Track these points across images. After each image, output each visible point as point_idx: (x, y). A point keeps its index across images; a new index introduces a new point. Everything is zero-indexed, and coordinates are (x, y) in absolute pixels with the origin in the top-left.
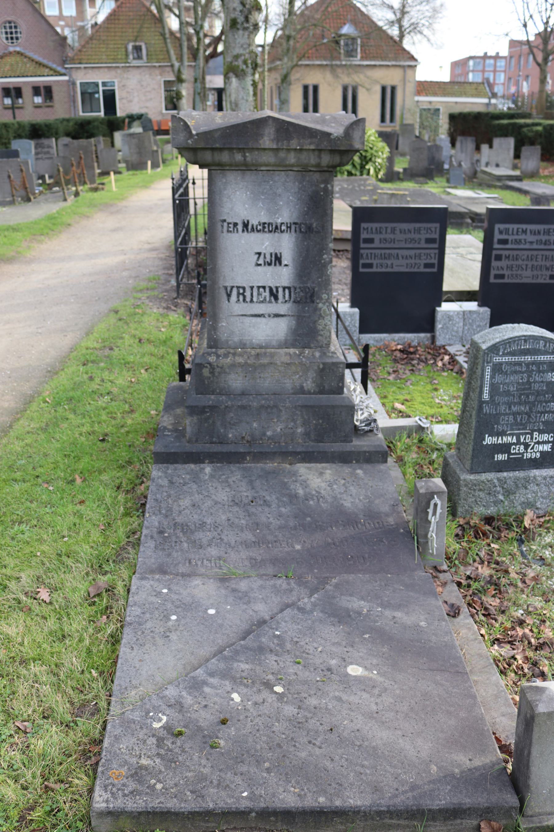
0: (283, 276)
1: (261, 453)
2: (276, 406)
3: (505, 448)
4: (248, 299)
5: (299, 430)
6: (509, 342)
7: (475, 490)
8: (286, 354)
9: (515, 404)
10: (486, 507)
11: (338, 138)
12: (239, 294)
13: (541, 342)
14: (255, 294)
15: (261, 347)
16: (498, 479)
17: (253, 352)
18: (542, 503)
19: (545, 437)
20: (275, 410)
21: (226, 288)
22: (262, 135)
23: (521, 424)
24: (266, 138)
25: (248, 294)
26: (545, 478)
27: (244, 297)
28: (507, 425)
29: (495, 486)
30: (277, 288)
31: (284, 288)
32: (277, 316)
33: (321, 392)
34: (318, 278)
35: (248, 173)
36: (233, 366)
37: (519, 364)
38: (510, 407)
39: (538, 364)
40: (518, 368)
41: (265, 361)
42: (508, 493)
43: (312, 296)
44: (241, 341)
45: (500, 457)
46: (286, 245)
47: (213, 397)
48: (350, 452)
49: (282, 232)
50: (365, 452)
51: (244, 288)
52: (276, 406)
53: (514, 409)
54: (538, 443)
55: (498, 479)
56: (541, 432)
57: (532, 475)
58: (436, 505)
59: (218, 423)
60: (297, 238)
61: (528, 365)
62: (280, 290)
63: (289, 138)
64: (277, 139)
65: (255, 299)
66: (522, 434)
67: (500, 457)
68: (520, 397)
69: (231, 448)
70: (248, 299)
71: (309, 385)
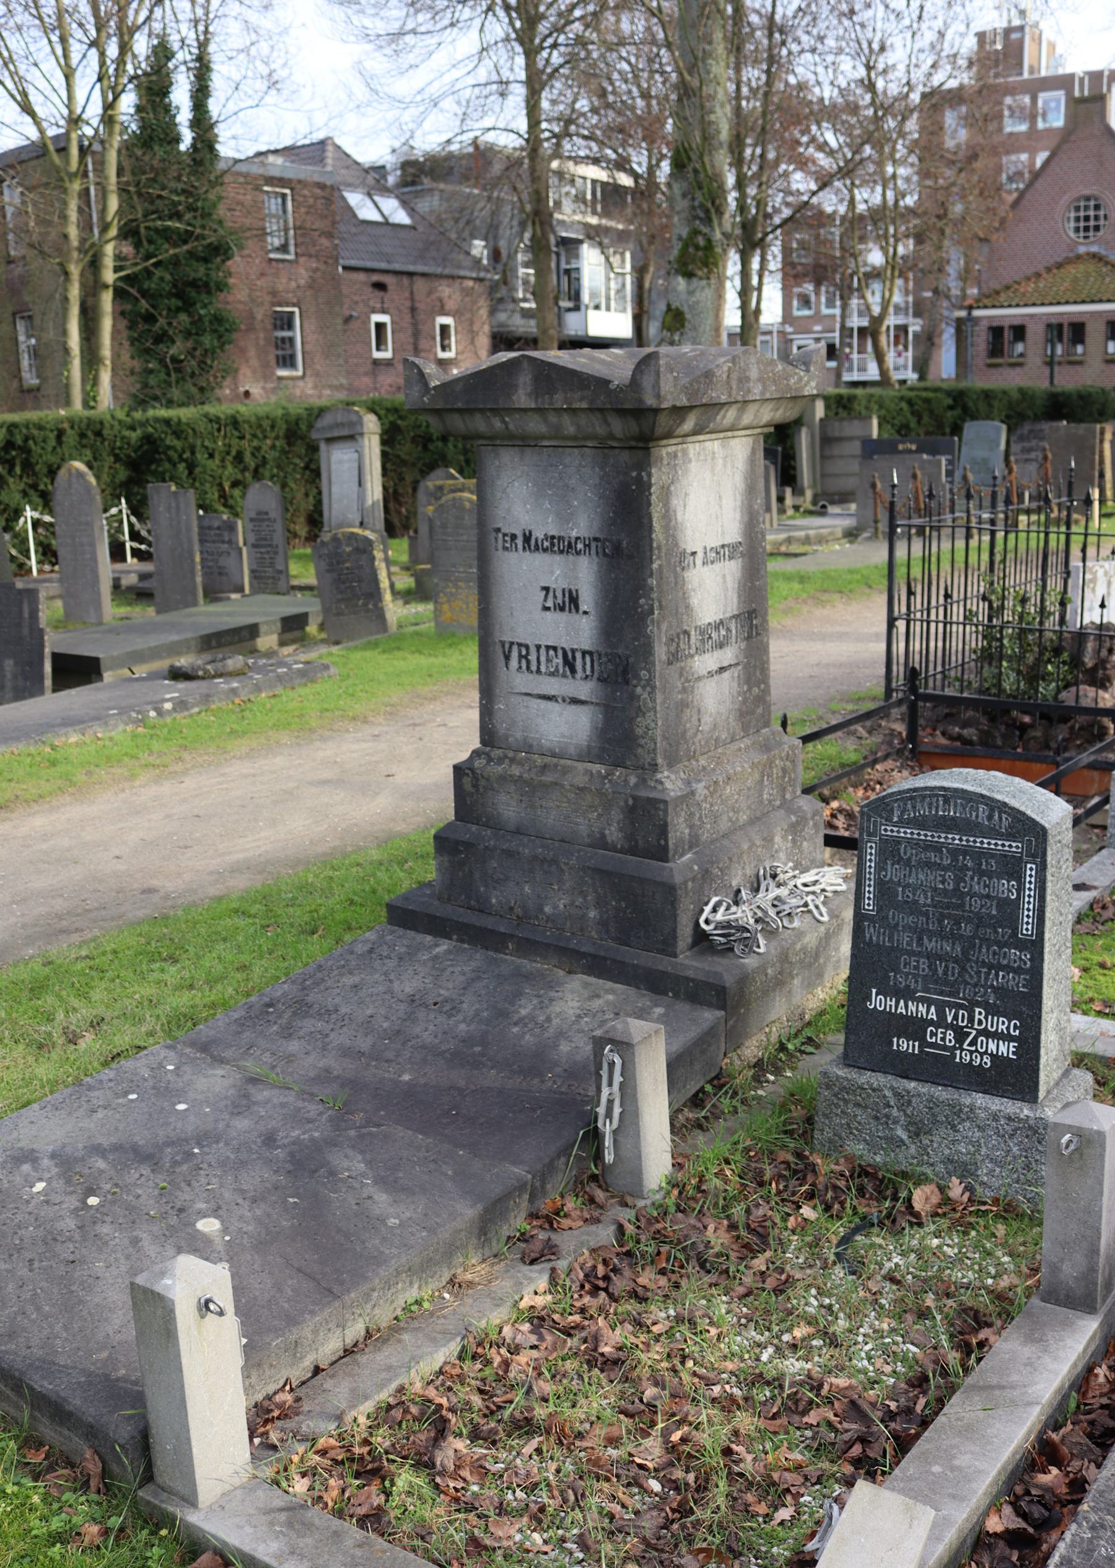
0: (580, 631)
1: (528, 940)
2: (554, 861)
3: (914, 1028)
4: (534, 668)
5: (592, 914)
6: (911, 798)
7: (846, 1101)
8: (587, 771)
9: (931, 935)
10: (873, 1147)
11: (620, 389)
12: (520, 656)
13: (981, 807)
14: (543, 659)
15: (554, 755)
16: (897, 1094)
17: (539, 761)
18: (991, 1173)
19: (1001, 1024)
20: (553, 868)
21: (503, 643)
22: (515, 387)
23: (946, 983)
24: (521, 392)
25: (533, 657)
26: (995, 1117)
27: (528, 662)
28: (915, 976)
29: (888, 1106)
30: (573, 651)
31: (584, 653)
32: (575, 701)
33: (633, 851)
34: (635, 639)
35: (528, 450)
36: (503, 778)
37: (937, 848)
38: (920, 940)
39: (980, 855)
40: (933, 857)
41: (548, 778)
42: (917, 1131)
43: (625, 672)
44: (525, 739)
45: (904, 1045)
46: (584, 575)
47: (474, 828)
48: (664, 973)
49: (578, 553)
50: (688, 979)
51: (527, 647)
52: (554, 861)
53: (930, 945)
54: (986, 1033)
55: (897, 1094)
56: (992, 1011)
57: (968, 1101)
58: (612, 1064)
59: (477, 875)
60: (600, 565)
61: (955, 852)
62: (578, 655)
63: (551, 391)
64: (536, 393)
65: (543, 669)
66: (951, 1005)
67: (904, 1045)
68: (940, 922)
69: (488, 922)
70: (534, 668)
71: (613, 834)
